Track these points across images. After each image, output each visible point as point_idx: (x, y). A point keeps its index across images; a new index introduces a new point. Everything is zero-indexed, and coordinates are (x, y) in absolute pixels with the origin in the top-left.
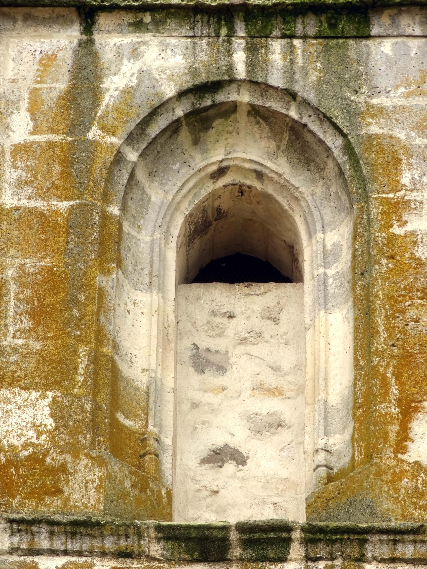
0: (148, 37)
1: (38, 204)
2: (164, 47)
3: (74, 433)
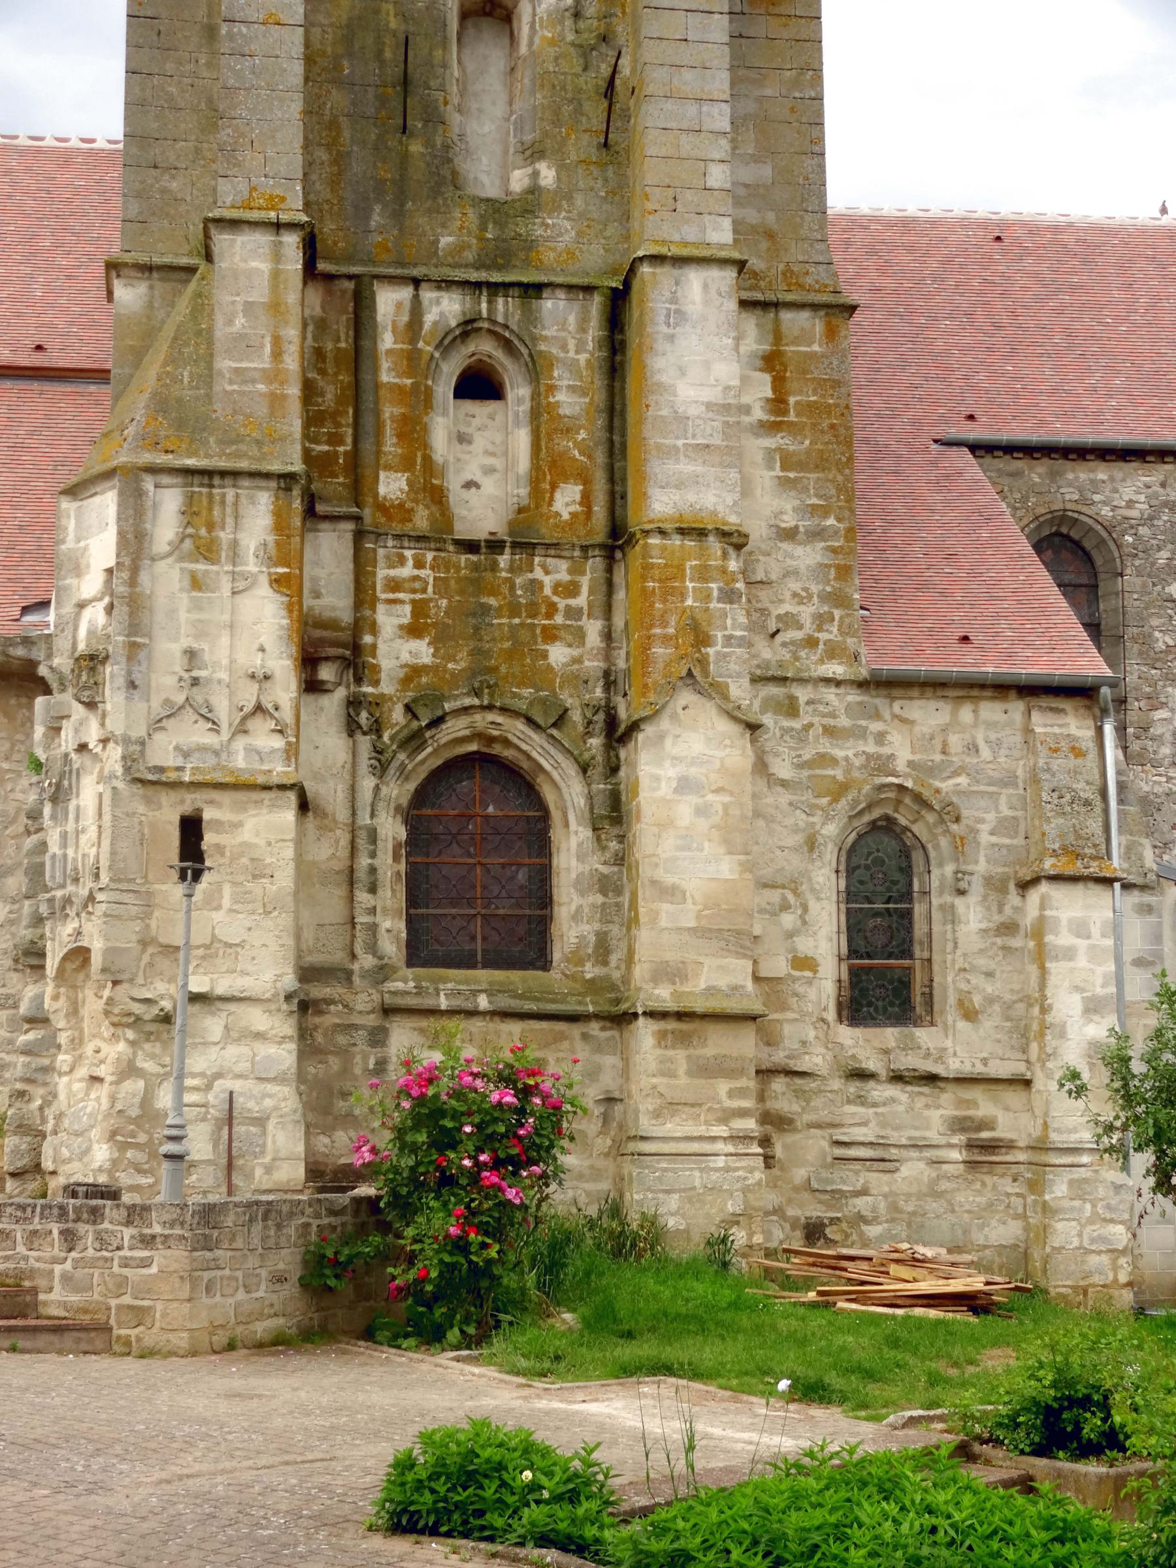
0: (443, 293)
1: (397, 380)
2: (451, 300)
3: (417, 493)
